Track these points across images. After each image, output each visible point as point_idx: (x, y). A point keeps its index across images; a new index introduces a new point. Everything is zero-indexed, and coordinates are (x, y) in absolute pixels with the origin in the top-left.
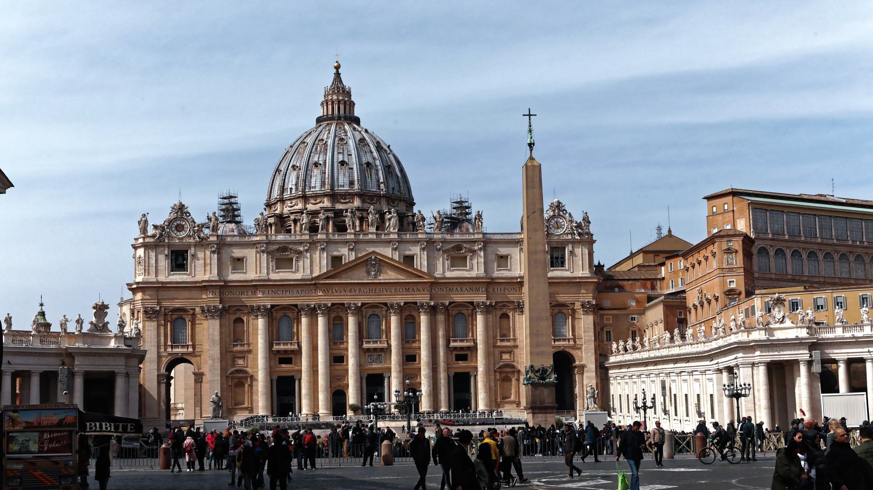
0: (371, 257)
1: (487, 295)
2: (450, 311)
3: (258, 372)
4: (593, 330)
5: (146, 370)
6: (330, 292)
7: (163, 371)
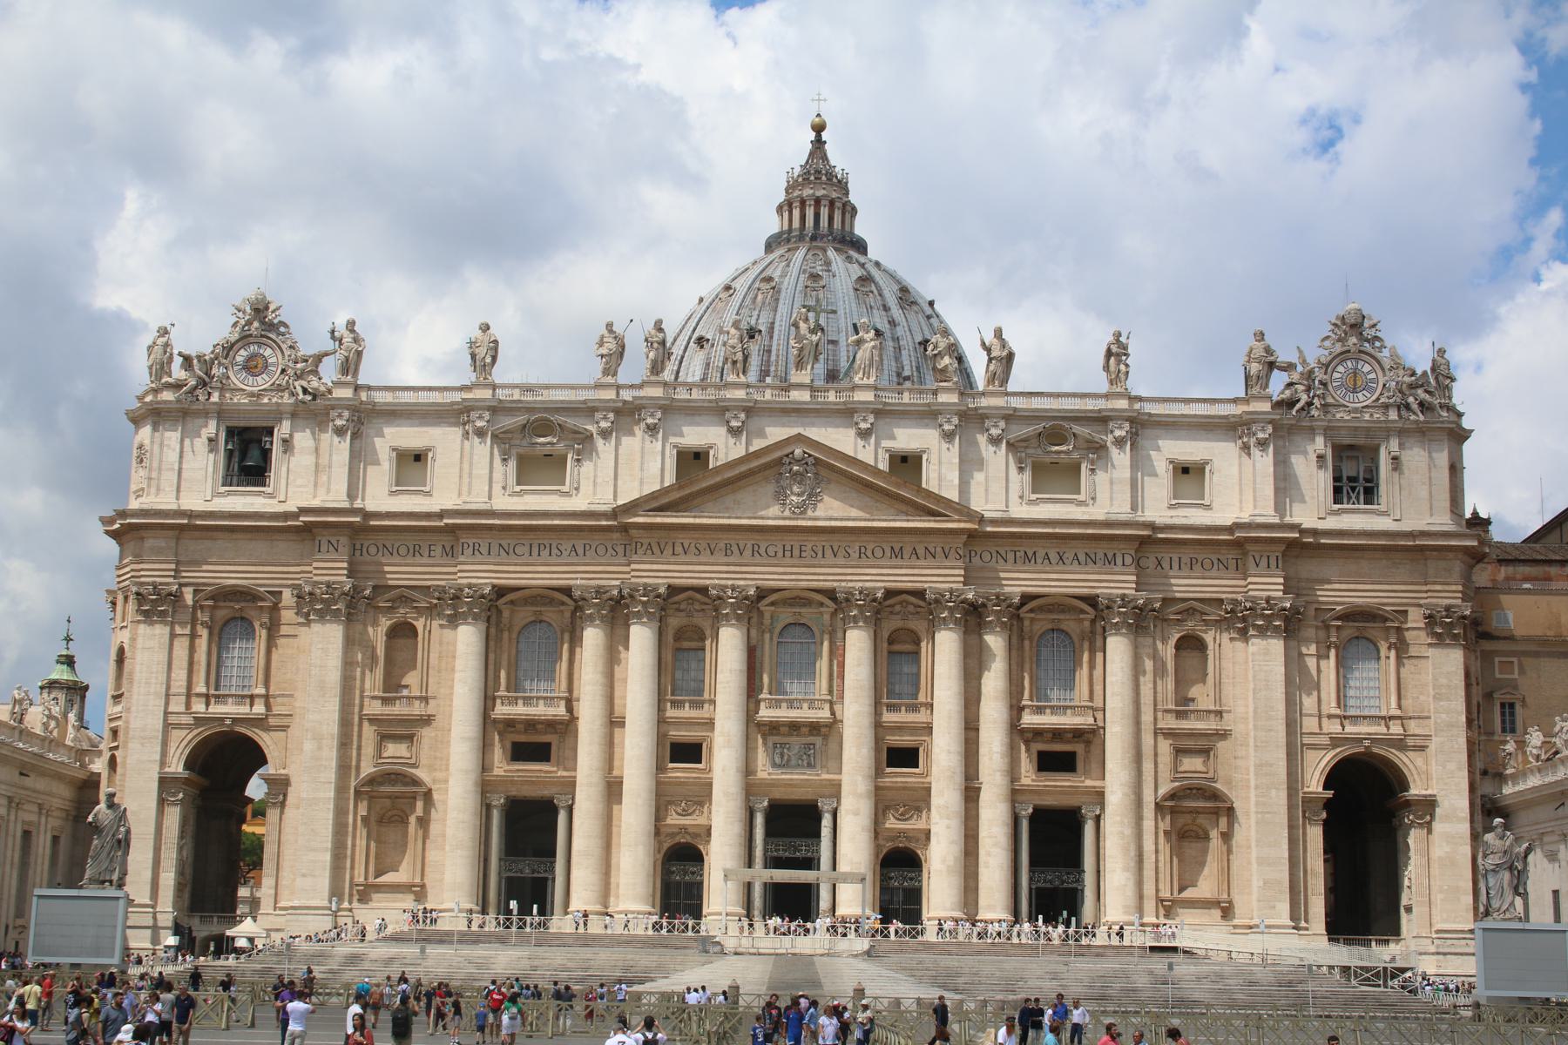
0: (792, 453)
1: (1137, 576)
2: (1027, 623)
3: (446, 781)
4: (1462, 693)
6: (669, 550)
7: (177, 767)
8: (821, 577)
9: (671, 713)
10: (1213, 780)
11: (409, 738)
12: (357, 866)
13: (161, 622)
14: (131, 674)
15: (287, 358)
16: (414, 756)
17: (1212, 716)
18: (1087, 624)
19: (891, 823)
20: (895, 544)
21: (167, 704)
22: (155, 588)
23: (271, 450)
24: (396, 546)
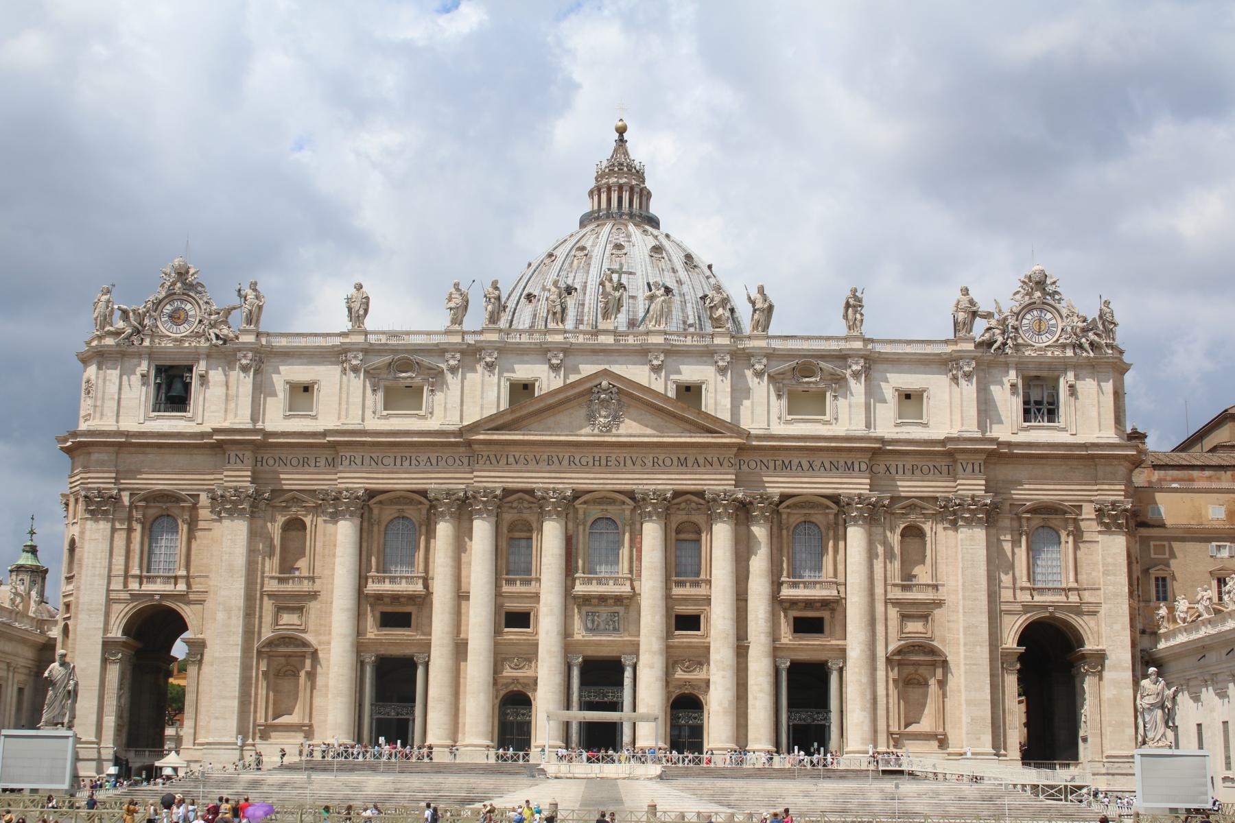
0: (600, 384)
2: (784, 516)
3: (329, 643)
4: (1126, 570)
5: (78, 629)
6: (503, 461)
7: (117, 633)
8: (623, 482)
9: (506, 588)
10: (931, 639)
11: (300, 610)
12: (259, 710)
13: (104, 520)
14: (80, 560)
15: (203, 311)
16: (304, 624)
17: (930, 589)
18: (831, 517)
19: (680, 674)
20: (681, 456)
21: (109, 583)
22: (99, 492)
23: (191, 383)
24: (289, 458)
